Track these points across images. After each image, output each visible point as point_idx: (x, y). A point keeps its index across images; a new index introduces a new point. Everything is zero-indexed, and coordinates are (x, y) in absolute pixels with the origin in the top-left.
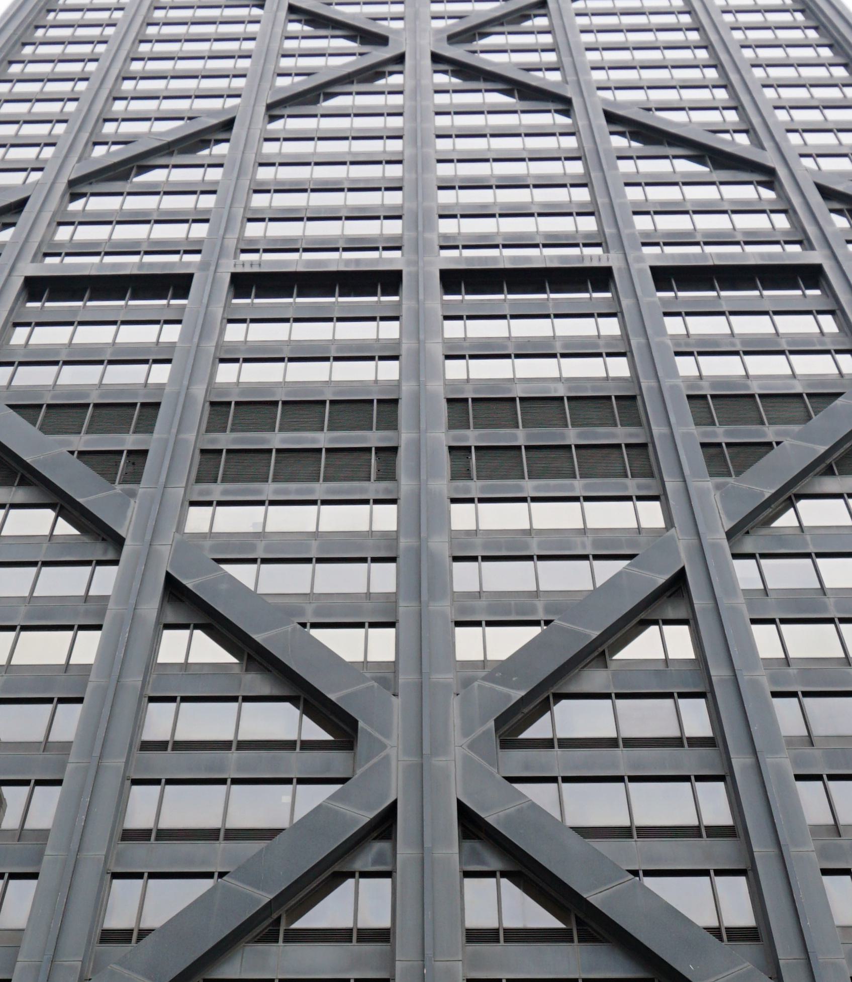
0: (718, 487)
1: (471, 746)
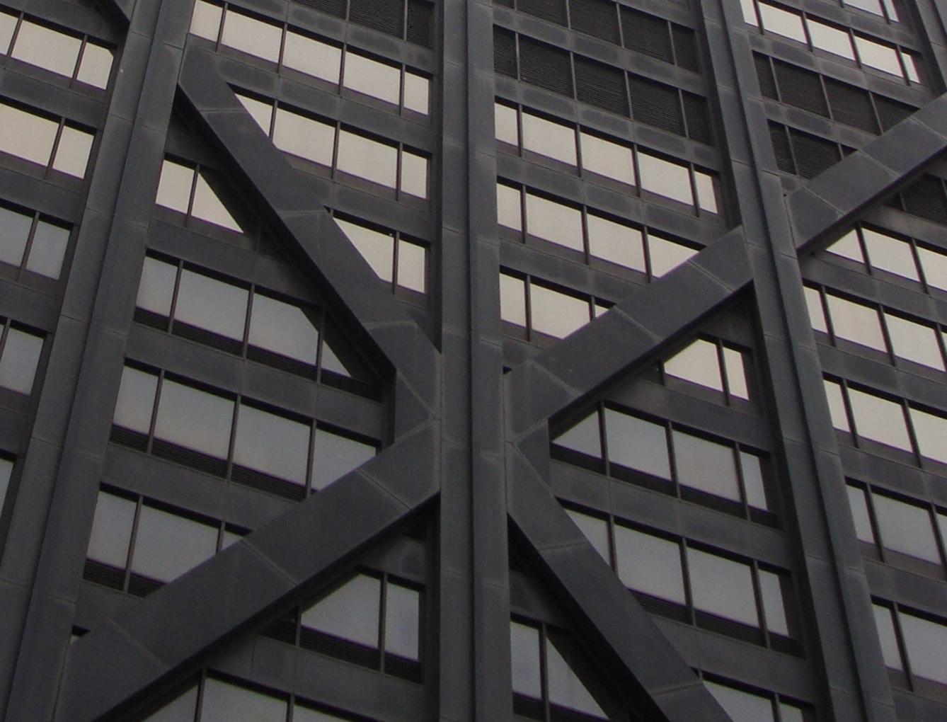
0: (787, 185)
1: (522, 446)
